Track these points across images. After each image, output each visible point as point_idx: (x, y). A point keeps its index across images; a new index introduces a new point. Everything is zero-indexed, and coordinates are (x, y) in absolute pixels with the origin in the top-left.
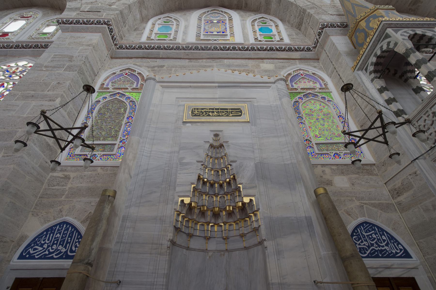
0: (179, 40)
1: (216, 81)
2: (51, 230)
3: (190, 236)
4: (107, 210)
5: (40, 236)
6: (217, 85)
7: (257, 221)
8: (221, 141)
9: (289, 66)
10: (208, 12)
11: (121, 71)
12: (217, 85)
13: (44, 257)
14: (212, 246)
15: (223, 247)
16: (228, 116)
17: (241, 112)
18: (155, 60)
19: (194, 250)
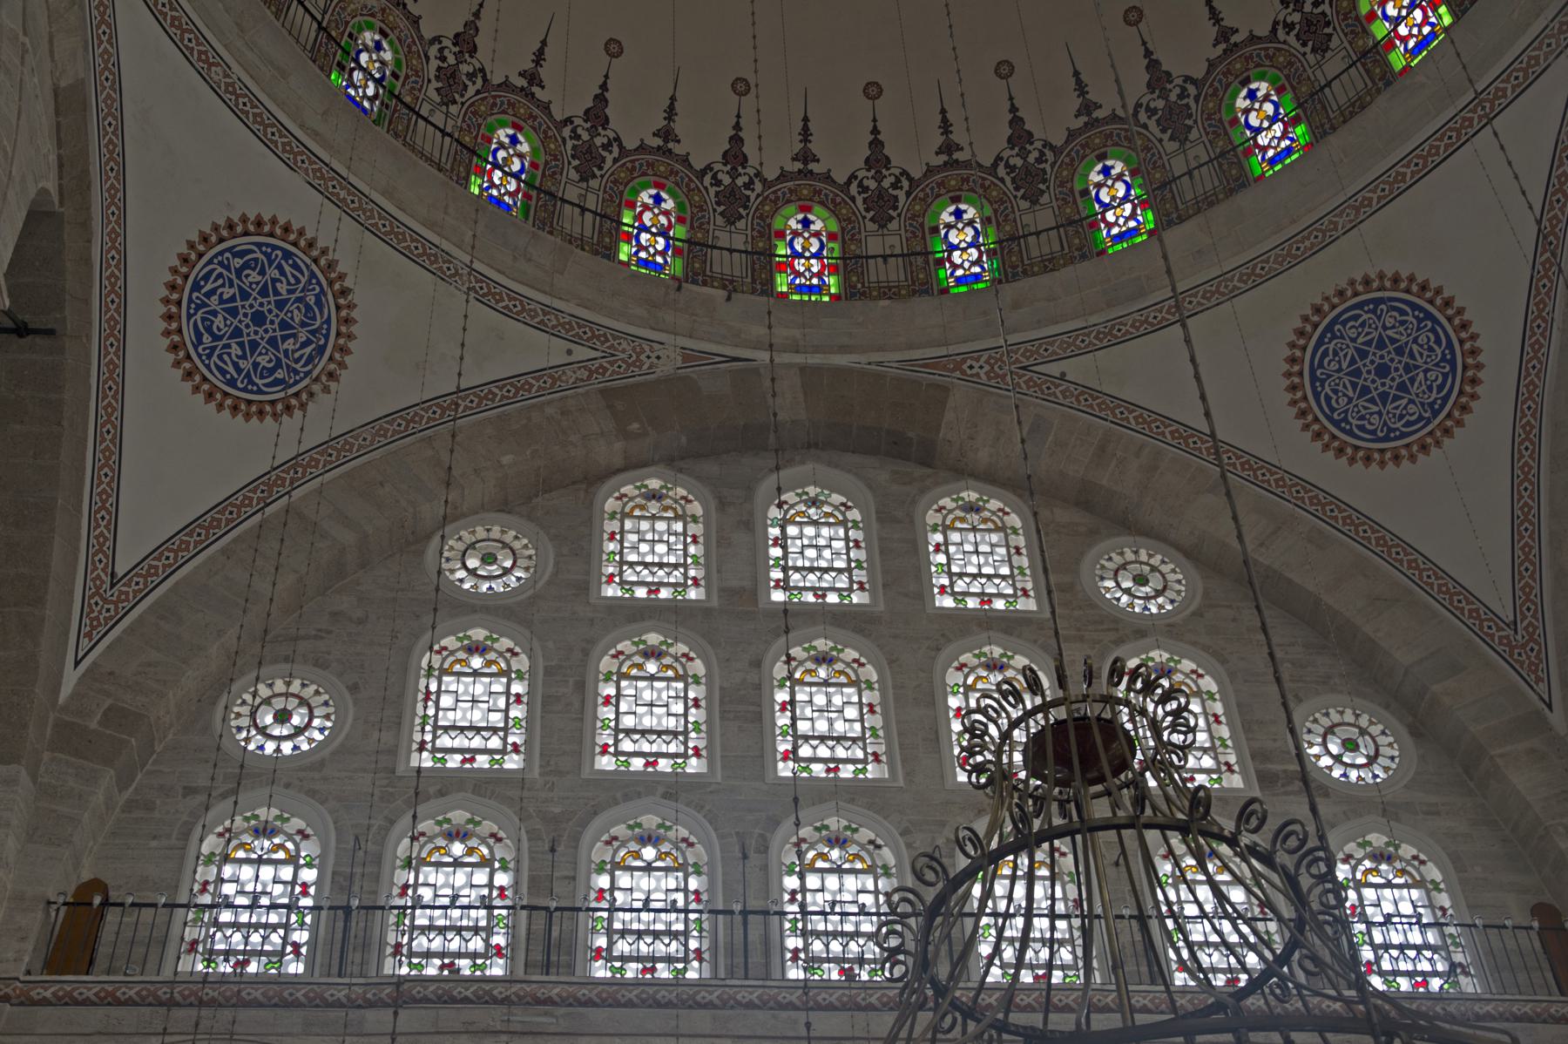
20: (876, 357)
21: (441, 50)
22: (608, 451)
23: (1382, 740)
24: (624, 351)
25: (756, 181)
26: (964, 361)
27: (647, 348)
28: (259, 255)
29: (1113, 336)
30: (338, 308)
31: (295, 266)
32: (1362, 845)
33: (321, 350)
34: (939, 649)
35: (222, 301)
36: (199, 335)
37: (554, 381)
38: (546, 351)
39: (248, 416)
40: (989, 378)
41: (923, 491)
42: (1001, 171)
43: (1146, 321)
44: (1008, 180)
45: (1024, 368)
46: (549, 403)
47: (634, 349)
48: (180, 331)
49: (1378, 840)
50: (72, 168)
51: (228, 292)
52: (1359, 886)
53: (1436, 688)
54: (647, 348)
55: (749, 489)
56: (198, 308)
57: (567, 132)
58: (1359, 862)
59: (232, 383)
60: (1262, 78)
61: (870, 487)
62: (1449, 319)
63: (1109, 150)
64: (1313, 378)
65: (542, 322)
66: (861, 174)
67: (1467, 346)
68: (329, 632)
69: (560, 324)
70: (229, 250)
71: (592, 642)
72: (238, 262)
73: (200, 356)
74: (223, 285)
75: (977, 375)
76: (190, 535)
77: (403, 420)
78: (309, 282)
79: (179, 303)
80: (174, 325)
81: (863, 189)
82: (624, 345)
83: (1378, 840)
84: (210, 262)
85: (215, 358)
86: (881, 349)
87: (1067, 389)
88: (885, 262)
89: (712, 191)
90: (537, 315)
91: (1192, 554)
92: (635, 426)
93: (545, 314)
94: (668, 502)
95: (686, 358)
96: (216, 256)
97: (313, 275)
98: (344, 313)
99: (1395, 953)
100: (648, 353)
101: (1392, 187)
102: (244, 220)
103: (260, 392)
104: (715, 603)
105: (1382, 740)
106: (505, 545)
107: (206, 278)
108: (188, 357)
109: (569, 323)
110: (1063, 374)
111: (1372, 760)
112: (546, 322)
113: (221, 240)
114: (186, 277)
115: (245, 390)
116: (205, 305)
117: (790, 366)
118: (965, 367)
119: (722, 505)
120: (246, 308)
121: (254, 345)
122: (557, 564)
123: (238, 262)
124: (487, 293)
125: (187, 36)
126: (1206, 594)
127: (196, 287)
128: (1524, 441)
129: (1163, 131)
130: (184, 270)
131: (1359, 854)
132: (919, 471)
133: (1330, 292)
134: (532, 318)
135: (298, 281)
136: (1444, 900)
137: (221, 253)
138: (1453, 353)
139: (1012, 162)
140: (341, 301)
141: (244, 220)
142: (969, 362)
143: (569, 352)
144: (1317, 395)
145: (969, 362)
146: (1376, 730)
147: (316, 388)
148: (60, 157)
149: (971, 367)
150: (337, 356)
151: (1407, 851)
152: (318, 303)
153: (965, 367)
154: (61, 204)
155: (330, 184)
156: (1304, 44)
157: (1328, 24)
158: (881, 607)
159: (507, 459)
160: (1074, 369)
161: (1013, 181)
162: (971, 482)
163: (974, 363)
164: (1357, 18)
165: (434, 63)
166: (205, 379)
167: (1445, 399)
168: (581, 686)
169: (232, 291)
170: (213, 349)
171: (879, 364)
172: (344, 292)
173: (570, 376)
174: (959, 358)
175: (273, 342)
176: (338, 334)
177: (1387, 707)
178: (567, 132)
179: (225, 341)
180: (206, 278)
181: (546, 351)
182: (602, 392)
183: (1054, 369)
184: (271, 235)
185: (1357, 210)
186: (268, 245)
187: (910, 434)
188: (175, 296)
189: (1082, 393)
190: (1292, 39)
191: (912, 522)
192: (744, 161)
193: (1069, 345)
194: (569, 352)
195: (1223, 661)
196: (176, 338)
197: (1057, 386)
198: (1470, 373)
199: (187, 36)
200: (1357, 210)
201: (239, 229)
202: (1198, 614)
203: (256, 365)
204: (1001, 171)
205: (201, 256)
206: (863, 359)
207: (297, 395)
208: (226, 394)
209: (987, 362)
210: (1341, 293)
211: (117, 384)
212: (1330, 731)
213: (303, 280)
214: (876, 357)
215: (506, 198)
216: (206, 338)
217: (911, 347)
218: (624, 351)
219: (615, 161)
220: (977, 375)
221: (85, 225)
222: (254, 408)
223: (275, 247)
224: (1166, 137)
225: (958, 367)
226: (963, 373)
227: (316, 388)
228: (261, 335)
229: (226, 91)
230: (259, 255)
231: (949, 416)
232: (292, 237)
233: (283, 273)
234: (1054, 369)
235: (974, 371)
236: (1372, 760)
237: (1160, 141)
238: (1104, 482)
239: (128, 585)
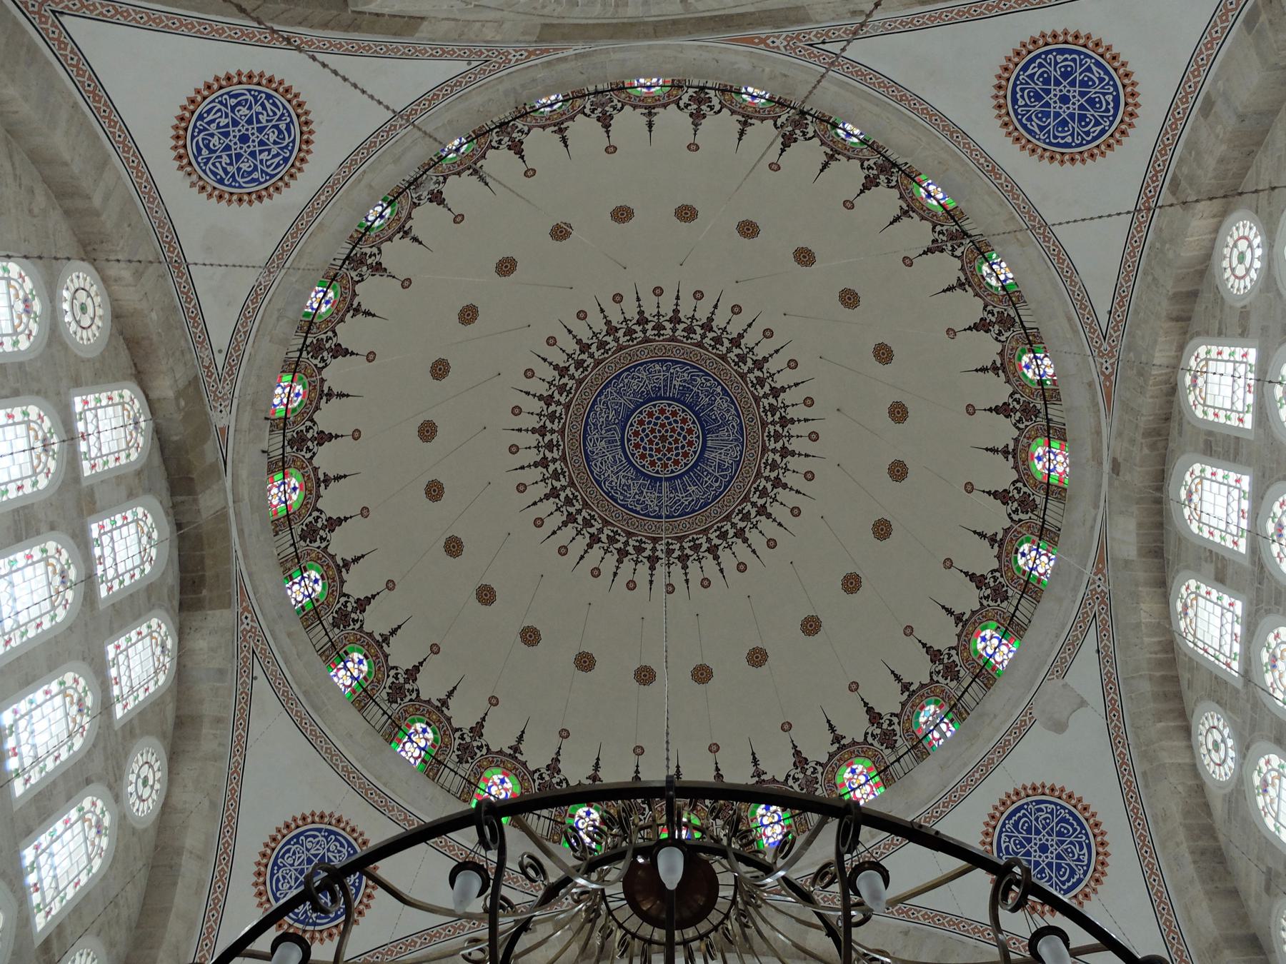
20: (240, 554)
21: (375, 255)
22: (165, 388)
24: (223, 388)
25: (311, 454)
26: (250, 612)
27: (226, 403)
28: (287, 141)
29: (287, 701)
30: (249, 194)
31: (278, 165)
33: (221, 181)
34: (84, 659)
35: (258, 114)
36: (236, 96)
37: (201, 343)
38: (220, 337)
39: (176, 128)
40: (242, 632)
41: (167, 610)
42: (343, 600)
44: (339, 605)
45: (254, 652)
46: (186, 340)
47: (225, 394)
48: (240, 83)
50: (377, 21)
51: (263, 118)
54: (226, 403)
55: (149, 490)
56: (255, 97)
57: (330, 334)
59: (201, 117)
60: (435, 733)
61: (163, 574)
63: (370, 659)
64: (297, 836)
65: (239, 331)
66: (323, 516)
68: (20, 186)
69: (238, 343)
70: (292, 121)
71: (46, 397)
72: (283, 126)
73: (222, 96)
74: (268, 115)
75: (243, 623)
76: (90, 78)
77: (169, 238)
78: (267, 174)
79: (259, 84)
80: (244, 79)
81: (316, 519)
82: (227, 388)
84: (284, 107)
85: (219, 106)
86: (245, 556)
87: (247, 684)
88: (291, 545)
89: (303, 428)
90: (244, 327)
91: (166, 807)
92: (182, 403)
93: (245, 333)
94: (134, 435)
95: (222, 429)
96: (288, 111)
97: (272, 176)
98: (246, 197)
100: (223, 404)
102: (311, 132)
103: (193, 137)
104: (84, 484)
106: (93, 319)
107: (274, 104)
108: (221, 88)
109: (239, 350)
110: (256, 678)
112: (239, 334)
113: (298, 116)
114: (276, 90)
115: (195, 126)
116: (256, 102)
117: (226, 499)
118: (246, 614)
119: (139, 473)
120: (252, 130)
121: (226, 135)
122: (88, 360)
123: (283, 126)
124: (256, 294)
125: (427, 103)
127: (269, 97)
129: (390, 688)
130: (281, 90)
132: (176, 603)
133: (352, 824)
134: (242, 325)
135: (268, 167)
137: (290, 115)
139: (349, 604)
140: (254, 196)
141: (311, 132)
142: (249, 616)
143: (220, 351)
144: (288, 843)
145: (249, 616)
147: (194, 177)
148: (383, 15)
149: (246, 618)
150: (216, 193)
152: (253, 180)
153: (246, 614)
154: (353, 12)
155: (330, 188)
156: (458, 750)
157: (472, 758)
158: (101, 607)
159: (154, 315)
160: (261, 684)
161: (340, 608)
162: (177, 641)
163: (249, 619)
164: (482, 773)
165: (368, 251)
166: (205, 98)
168: (16, 393)
169: (264, 121)
170: (226, 106)
171: (237, 558)
172: (260, 198)
173: (205, 354)
174: (250, 608)
175: (228, 148)
176: (231, 194)
178: (330, 334)
179: (230, 114)
180: (274, 104)
181: (220, 337)
182: (196, 378)
183: (258, 671)
184: (300, 150)
185: (405, 819)
186: (293, 147)
187: (205, 592)
188: (264, 82)
189: (247, 695)
190: (458, 741)
191: (150, 610)
192: (320, 444)
193: (275, 676)
194: (220, 351)
196: (235, 80)
197: (247, 677)
199: (427, 103)
201: (305, 129)
203: (275, 143)
204: (343, 600)
205: (289, 101)
206: (238, 547)
207: (190, 164)
208: (193, 113)
209: (252, 627)
210: (353, 830)
211: (208, 34)
213: (268, 171)
214: (240, 554)
215: (309, 302)
216: (233, 101)
217: (250, 575)
218: (223, 388)
219: (316, 365)
220: (243, 623)
221: (325, 26)
222: (181, 132)
223: (291, 152)
224: (388, 690)
225: (246, 609)
226: (242, 614)
227: (194, 177)
228: (233, 140)
229: (391, 125)
230: (287, 141)
231: (218, 612)
232: (297, 164)
233: (274, 157)
234: (258, 671)
235: (244, 620)
238: (204, 731)
239: (53, 25)
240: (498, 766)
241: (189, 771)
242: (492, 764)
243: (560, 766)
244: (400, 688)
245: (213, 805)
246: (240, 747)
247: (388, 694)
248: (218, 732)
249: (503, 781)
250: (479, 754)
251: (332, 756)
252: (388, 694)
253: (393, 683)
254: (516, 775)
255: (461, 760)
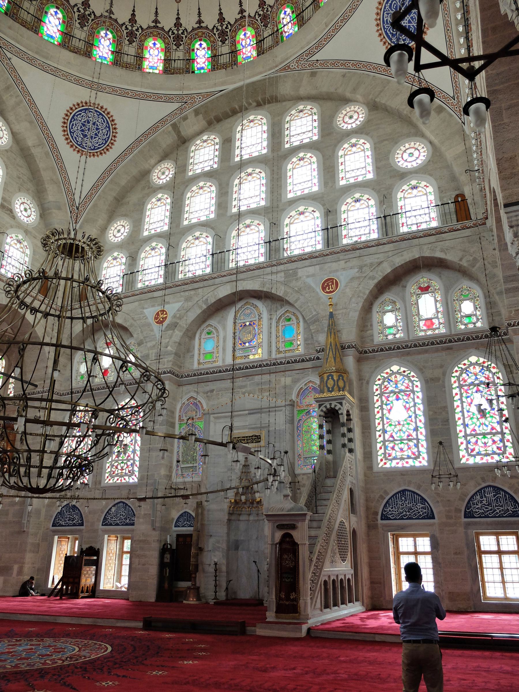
0: (220, 363)
1: (246, 409)
2: (181, 515)
3: (240, 515)
4: (200, 511)
5: (179, 518)
6: (247, 412)
7: (262, 510)
8: (248, 463)
9: (303, 378)
10: (241, 307)
11: (188, 400)
12: (247, 412)
13: (183, 526)
14: (251, 518)
15: (256, 518)
16: (252, 442)
17: (260, 438)
18: (207, 383)
19: (242, 520)
23: (33, 213)
29: (31, 61)
32: (16, 236)
43: (43, 66)
49: (20, 237)
52: (10, 246)
53: (54, 211)
58: (14, 240)
60: (112, 33)
62: (113, 132)
64: (73, 117)
67: (112, 141)
83: (20, 237)
91: (14, 134)
99: (11, 266)
101: (124, 93)
105: (33, 213)
111: (29, 216)
126: (11, 147)
128: (108, 172)
131: (14, 238)
136: (27, 259)
138: (108, 140)
146: (33, 210)
151: (25, 243)
156: (127, 36)
157: (136, 38)
160: (15, 61)
164: (143, 44)
167: (99, 148)
177: (38, 206)
183: (9, 55)
185: (113, 91)
189: (12, 68)
190: (125, 32)
195: (7, 168)
198: (108, 147)
200: (113, 91)
202: (7, 151)
212: (23, 203)
224: (78, 21)
234: (9, 55)
236: (29, 216)
237: (76, 21)
238: (4, 98)
240: (150, 36)
241: (12, 118)
242: (147, 36)
243: (181, 22)
244: (84, 16)
245: (31, 122)
246: (26, 93)
247: (79, 23)
248: (12, 93)
249: (154, 44)
250: (138, 34)
251: (67, 76)
252: (79, 23)
253: (79, 15)
254: (160, 37)
255: (131, 42)
